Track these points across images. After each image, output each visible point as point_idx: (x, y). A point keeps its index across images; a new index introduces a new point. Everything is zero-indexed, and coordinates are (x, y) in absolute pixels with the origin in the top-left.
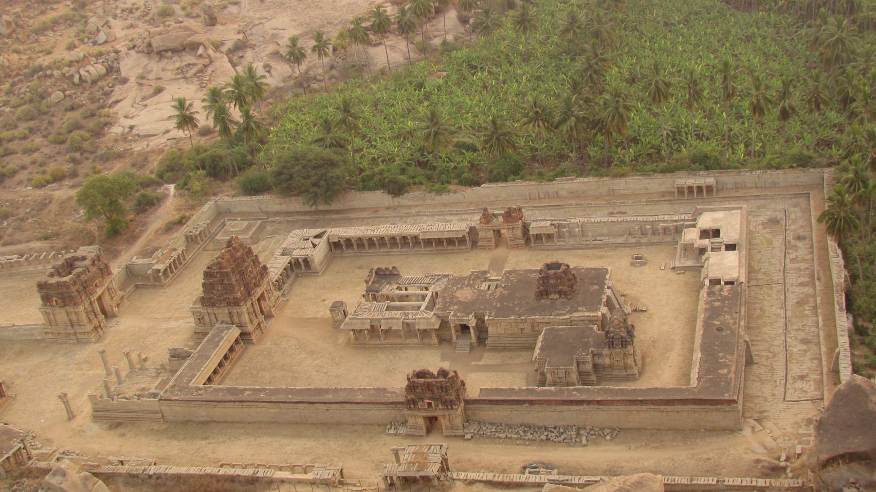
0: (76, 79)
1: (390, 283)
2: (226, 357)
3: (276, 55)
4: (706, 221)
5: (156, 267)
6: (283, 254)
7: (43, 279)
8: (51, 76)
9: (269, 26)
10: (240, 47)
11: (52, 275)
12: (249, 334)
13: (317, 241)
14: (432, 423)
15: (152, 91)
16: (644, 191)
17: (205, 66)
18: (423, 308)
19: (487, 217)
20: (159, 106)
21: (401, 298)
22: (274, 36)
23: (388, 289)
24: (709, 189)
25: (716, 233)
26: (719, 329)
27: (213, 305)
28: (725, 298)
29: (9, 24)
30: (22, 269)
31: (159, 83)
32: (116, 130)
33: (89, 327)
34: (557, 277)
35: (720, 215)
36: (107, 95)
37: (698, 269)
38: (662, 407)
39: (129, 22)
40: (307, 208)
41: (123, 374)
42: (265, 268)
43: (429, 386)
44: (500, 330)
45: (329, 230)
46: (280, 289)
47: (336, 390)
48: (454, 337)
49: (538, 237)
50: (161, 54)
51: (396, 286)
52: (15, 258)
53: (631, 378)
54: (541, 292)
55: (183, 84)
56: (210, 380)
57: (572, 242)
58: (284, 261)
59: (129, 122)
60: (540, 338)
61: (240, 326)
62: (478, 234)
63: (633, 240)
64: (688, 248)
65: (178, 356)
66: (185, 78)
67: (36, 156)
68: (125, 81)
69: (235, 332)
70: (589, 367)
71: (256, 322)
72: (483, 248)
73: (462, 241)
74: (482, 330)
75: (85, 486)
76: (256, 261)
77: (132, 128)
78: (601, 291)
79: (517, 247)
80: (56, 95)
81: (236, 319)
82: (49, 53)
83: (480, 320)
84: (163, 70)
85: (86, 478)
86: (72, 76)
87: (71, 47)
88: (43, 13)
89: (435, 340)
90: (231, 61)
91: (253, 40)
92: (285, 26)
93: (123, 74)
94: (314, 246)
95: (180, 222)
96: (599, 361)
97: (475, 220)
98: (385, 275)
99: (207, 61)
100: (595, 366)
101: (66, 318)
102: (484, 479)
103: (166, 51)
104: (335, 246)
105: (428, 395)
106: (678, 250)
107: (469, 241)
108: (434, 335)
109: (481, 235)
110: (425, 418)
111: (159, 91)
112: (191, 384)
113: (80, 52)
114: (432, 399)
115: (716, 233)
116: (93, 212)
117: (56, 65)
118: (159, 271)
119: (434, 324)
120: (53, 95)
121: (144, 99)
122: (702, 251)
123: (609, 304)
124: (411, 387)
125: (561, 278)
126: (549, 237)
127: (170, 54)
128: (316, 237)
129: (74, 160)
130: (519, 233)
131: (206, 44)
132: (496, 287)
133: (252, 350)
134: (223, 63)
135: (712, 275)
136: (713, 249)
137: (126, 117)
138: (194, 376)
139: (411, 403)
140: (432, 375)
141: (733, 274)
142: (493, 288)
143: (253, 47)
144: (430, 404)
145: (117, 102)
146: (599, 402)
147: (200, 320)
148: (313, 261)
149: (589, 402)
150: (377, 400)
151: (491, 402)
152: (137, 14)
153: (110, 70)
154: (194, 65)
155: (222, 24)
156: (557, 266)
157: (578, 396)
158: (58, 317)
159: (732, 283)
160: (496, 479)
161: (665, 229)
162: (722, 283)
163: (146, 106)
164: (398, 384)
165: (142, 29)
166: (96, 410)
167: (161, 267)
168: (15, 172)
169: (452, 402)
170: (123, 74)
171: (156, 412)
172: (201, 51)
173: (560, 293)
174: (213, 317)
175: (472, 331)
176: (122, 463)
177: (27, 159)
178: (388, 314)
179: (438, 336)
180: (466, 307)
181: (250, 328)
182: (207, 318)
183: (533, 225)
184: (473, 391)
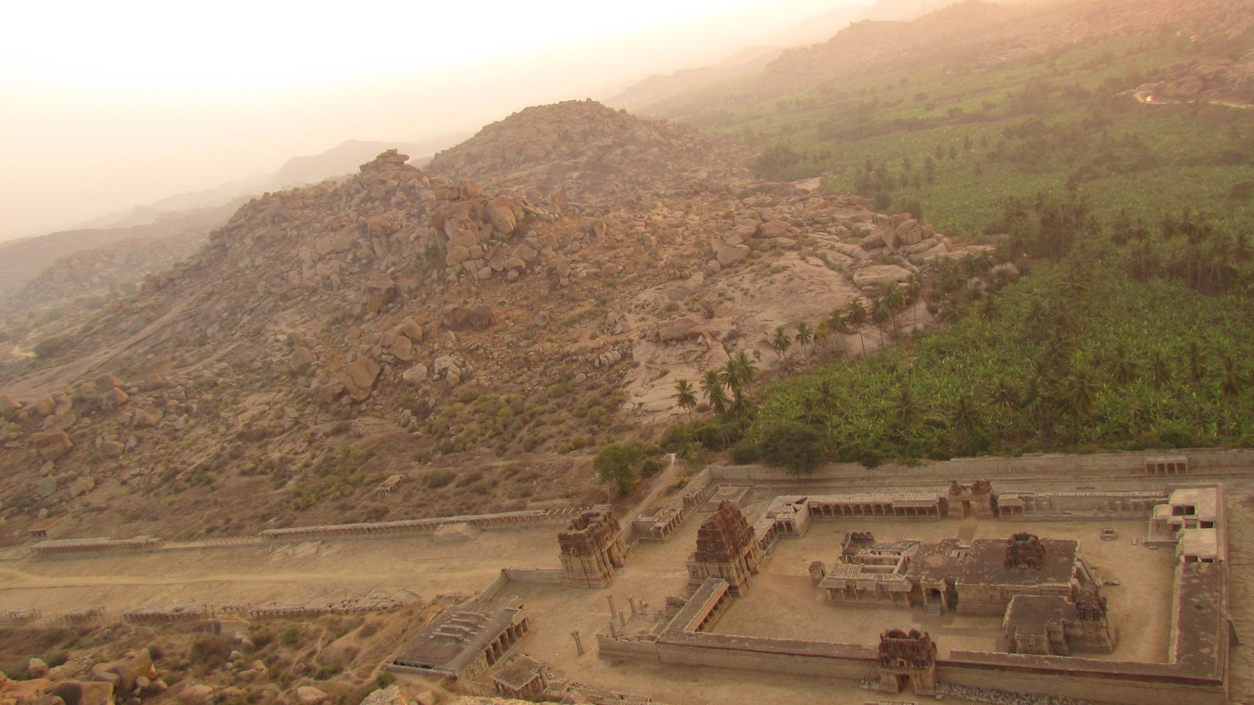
0: (597, 364)
2: (715, 608)
3: (765, 343)
4: (1180, 497)
5: (658, 525)
6: (768, 517)
7: (563, 531)
9: (758, 318)
10: (733, 336)
11: (571, 528)
12: (736, 588)
13: (797, 507)
14: (904, 683)
19: (956, 489)
21: (875, 561)
22: (763, 327)
23: (862, 553)
24: (1181, 467)
25: (1191, 510)
26: (1199, 607)
27: (706, 560)
28: (1205, 576)
29: (544, 317)
30: (546, 522)
31: (665, 367)
32: (628, 406)
33: (600, 575)
34: (1025, 547)
35: (1194, 492)
36: (622, 376)
37: (1172, 545)
38: (1140, 683)
40: (790, 477)
41: (626, 617)
42: (752, 529)
43: (901, 645)
44: (970, 596)
46: (764, 548)
47: (814, 644)
50: (667, 343)
52: (541, 512)
53: (1105, 651)
55: (686, 369)
56: (701, 628)
57: (1040, 515)
58: (769, 523)
60: (1010, 605)
61: (729, 580)
63: (1103, 515)
64: (1161, 524)
65: (674, 604)
67: (562, 427)
68: (636, 365)
69: (724, 586)
70: (1060, 637)
72: (953, 517)
73: (932, 510)
74: (952, 595)
76: (744, 523)
77: (641, 404)
78: (1071, 563)
79: (987, 518)
80: (581, 377)
81: (725, 574)
82: (575, 341)
83: (950, 585)
87: (593, 337)
88: (572, 309)
89: (907, 603)
90: (725, 348)
92: (772, 318)
94: (796, 511)
95: (680, 486)
96: (1073, 632)
97: (945, 491)
98: (861, 540)
99: (705, 348)
100: (1067, 637)
101: (580, 566)
104: (817, 513)
105: (900, 654)
106: (1150, 527)
107: (939, 511)
109: (951, 505)
111: (664, 373)
112: (684, 630)
113: (600, 341)
114: (903, 656)
115: (1191, 510)
116: (606, 476)
117: (581, 352)
121: (651, 380)
122: (1176, 527)
123: (1079, 575)
124: (884, 646)
126: (1017, 509)
129: (592, 432)
130: (987, 504)
133: (739, 603)
135: (1188, 551)
136: (1187, 526)
139: (884, 661)
140: (904, 636)
141: (1212, 552)
142: (962, 556)
143: (744, 336)
144: (902, 664)
146: (1072, 673)
147: (694, 573)
149: (1061, 672)
150: (852, 656)
151: (961, 665)
152: (649, 309)
153: (625, 356)
156: (1025, 537)
157: (1050, 666)
159: (1209, 560)
161: (1136, 506)
164: (872, 642)
165: (652, 321)
166: (602, 648)
167: (662, 525)
168: (544, 440)
169: (923, 663)
171: (651, 653)
172: (700, 339)
173: (1029, 563)
176: (622, 697)
177: (554, 430)
178: (862, 576)
179: (910, 599)
180: (936, 572)
181: (737, 583)
183: (1001, 497)
184: (943, 654)
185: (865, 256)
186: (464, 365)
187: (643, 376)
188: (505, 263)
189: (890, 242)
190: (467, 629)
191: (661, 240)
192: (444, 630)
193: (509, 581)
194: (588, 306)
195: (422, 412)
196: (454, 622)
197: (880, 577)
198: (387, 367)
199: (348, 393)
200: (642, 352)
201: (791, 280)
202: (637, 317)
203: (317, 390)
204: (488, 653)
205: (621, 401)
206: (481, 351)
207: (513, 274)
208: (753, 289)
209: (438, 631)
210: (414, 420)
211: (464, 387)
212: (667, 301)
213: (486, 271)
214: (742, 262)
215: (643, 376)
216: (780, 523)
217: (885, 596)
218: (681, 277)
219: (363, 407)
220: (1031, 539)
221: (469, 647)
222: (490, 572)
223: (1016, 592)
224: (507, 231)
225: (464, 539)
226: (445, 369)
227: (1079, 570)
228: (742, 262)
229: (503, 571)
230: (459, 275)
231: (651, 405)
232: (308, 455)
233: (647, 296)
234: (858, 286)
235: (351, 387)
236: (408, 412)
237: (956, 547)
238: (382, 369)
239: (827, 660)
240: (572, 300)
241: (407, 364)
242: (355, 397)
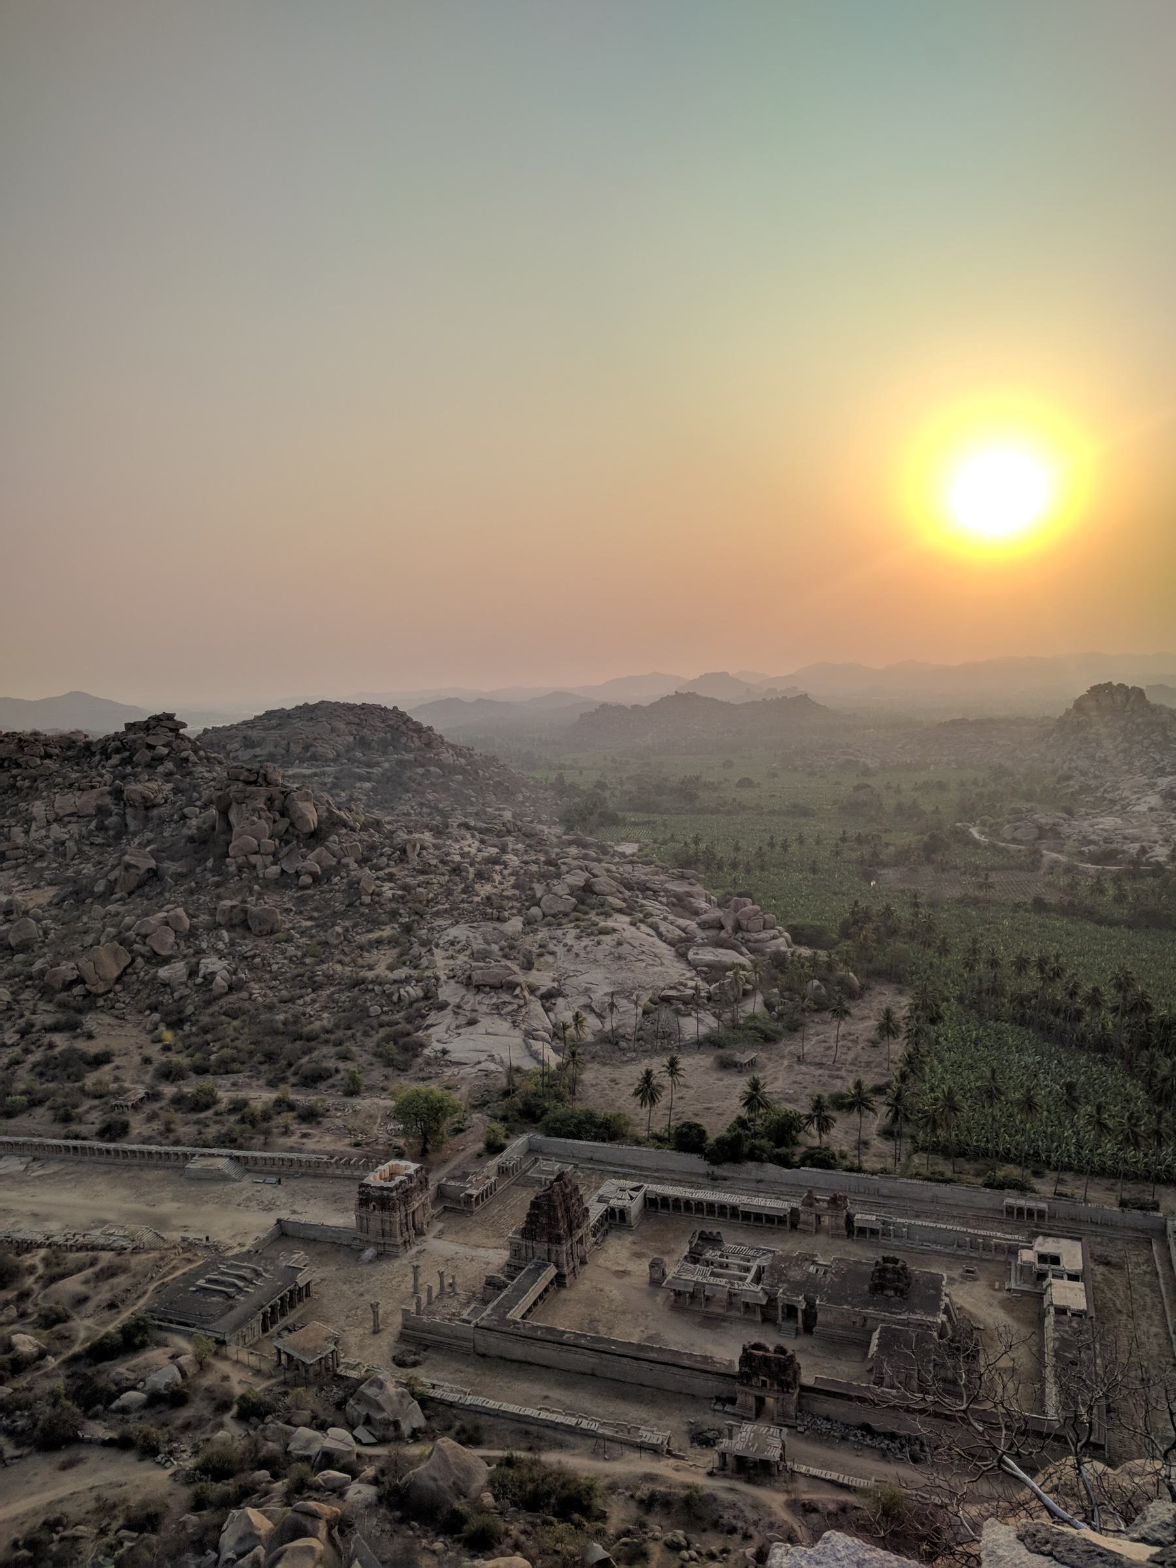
0: (395, 998)
4: (1048, 1246)
5: (469, 1192)
6: (599, 1201)
9: (582, 980)
12: (564, 1276)
16: (969, 1204)
17: (520, 1007)
18: (749, 1280)
19: (810, 1202)
22: (587, 990)
23: (710, 1254)
25: (1056, 1260)
27: (534, 1239)
29: (339, 935)
30: (329, 1171)
33: (400, 1240)
34: (895, 1272)
36: (424, 1017)
37: (1040, 1296)
39: (450, 953)
41: (434, 1295)
42: (587, 1210)
43: (766, 1360)
44: (830, 1318)
45: (646, 1185)
46: (594, 1236)
48: (780, 1318)
49: (862, 1231)
50: (479, 988)
51: (719, 1253)
52: (325, 1158)
54: (876, 1285)
55: (498, 1021)
56: (523, 1317)
57: (896, 1242)
59: (439, 1047)
60: (876, 1335)
61: (557, 1267)
62: (799, 1216)
63: (963, 1253)
64: (1025, 1269)
65: (494, 1285)
66: (500, 1014)
68: (442, 1007)
69: (551, 1272)
72: (804, 1231)
73: (781, 1220)
74: (810, 1315)
75: (401, 1403)
76: (580, 1200)
79: (838, 1236)
81: (553, 1258)
85: (403, 1395)
86: (392, 994)
87: (391, 968)
88: (370, 931)
89: (759, 1318)
90: (543, 1006)
91: (567, 990)
94: (632, 1198)
97: (796, 1204)
98: (712, 1240)
99: (522, 1002)
102: (828, 1477)
103: (485, 986)
106: (1013, 1272)
107: (788, 1223)
108: (758, 1309)
109: (803, 1217)
110: (756, 1397)
111: (472, 1023)
112: (508, 1316)
113: (402, 973)
115: (1056, 1260)
118: (471, 1196)
119: (760, 1299)
121: (458, 1027)
122: (1042, 1276)
123: (947, 1311)
125: (899, 1274)
126: (874, 1232)
127: (488, 989)
128: (633, 1189)
130: (842, 1222)
131: (524, 985)
132: (825, 1273)
133: (564, 1294)
134: (536, 1006)
136: (1054, 1276)
138: (511, 1308)
142: (821, 1272)
143: (565, 996)
144: (764, 1383)
147: (516, 1253)
148: (629, 1213)
152: (458, 947)
153: (426, 997)
154: (510, 1003)
155: (538, 970)
156: (896, 1261)
158: (371, 1224)
160: (841, 1481)
161: (997, 1246)
162: (1069, 1314)
166: (405, 1327)
172: (518, 991)
173: (896, 1289)
174: (530, 1251)
175: (800, 1314)
176: (434, 1386)
178: (712, 1280)
179: (763, 1313)
180: (796, 1287)
181: (566, 1270)
182: (523, 1251)
183: (858, 1216)
185: (700, 934)
188: (299, 865)
189: (729, 925)
190: (241, 1284)
191: (480, 876)
192: (209, 1281)
193: (284, 1233)
194: (387, 932)
197: (732, 1284)
198: (139, 960)
199: (84, 982)
200: (448, 992)
201: (620, 944)
202: (447, 954)
203: (42, 973)
204: (264, 1314)
206: (258, 960)
207: (306, 880)
208: (578, 946)
209: (201, 1282)
211: (232, 998)
213: (274, 870)
214: (566, 915)
216: (613, 1209)
217: (739, 1310)
218: (498, 919)
219: (101, 1002)
220: (900, 1264)
221: (243, 1304)
222: (259, 1223)
223: (883, 1321)
224: (306, 830)
225: (225, 1178)
226: (213, 973)
227: (947, 1305)
228: (566, 915)
229: (279, 1221)
230: (240, 870)
231: (454, 1056)
232: (18, 1049)
233: (459, 932)
235: (90, 976)
237: (814, 1263)
238: (133, 961)
239: (674, 1368)
240: (373, 921)
241: (166, 961)
242: (93, 989)
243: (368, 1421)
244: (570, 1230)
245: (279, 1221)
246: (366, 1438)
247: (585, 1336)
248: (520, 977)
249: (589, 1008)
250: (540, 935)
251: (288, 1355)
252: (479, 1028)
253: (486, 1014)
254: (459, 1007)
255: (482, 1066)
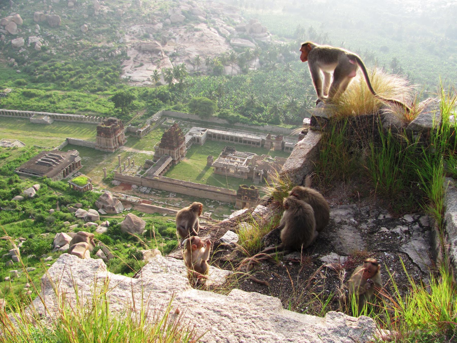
0: (110, 55)
1: (232, 153)
3: (188, 61)
6: (189, 135)
8: (100, 51)
13: (203, 132)
15: (139, 64)
18: (243, 164)
19: (269, 138)
20: (141, 71)
22: (188, 54)
27: (164, 147)
31: (142, 62)
32: (123, 77)
33: (113, 147)
36: (121, 63)
42: (185, 138)
45: (208, 129)
55: (152, 65)
56: (159, 175)
61: (172, 157)
65: (149, 164)
66: (152, 62)
68: (129, 59)
69: (170, 159)
71: (178, 157)
73: (258, 144)
76: (182, 135)
77: (130, 77)
80: (102, 59)
81: (171, 154)
82: (100, 42)
83: (265, 172)
84: (144, 58)
86: (108, 53)
88: (99, 27)
93: (128, 56)
94: (202, 134)
97: (264, 138)
101: (105, 142)
103: (146, 51)
104: (209, 136)
109: (266, 143)
111: (142, 65)
118: (140, 132)
120: (100, 59)
121: (135, 67)
127: (148, 52)
130: (280, 145)
134: (168, 60)
137: (128, 73)
145: (125, 66)
147: (157, 152)
148: (201, 139)
152: (136, 34)
154: (156, 58)
163: (136, 70)
165: (137, 41)
170: (128, 56)
172: (160, 53)
174: (162, 152)
179: (248, 176)
180: (261, 167)
181: (176, 159)
182: (160, 152)
183: (286, 143)
186: (44, 42)
187: (131, 64)
190: (54, 161)
192: (42, 160)
195: (20, 61)
196: (47, 157)
200: (131, 53)
202: (130, 37)
205: (121, 74)
206: (53, 38)
208: (185, 36)
209: (40, 160)
210: (16, 64)
212: (145, 33)
214: (181, 23)
215: (131, 64)
216: (195, 138)
229: (67, 139)
234: (232, 46)
236: (13, 60)
239: (214, 193)
240: (99, 23)
241: (15, 37)
243: (103, 207)
244: (178, 146)
245: (67, 139)
246: (103, 212)
247: (182, 181)
248: (161, 48)
249: (188, 61)
250: (170, 31)
251: (73, 185)
252: (145, 67)
253: (147, 62)
254: (136, 59)
255: (145, 82)
